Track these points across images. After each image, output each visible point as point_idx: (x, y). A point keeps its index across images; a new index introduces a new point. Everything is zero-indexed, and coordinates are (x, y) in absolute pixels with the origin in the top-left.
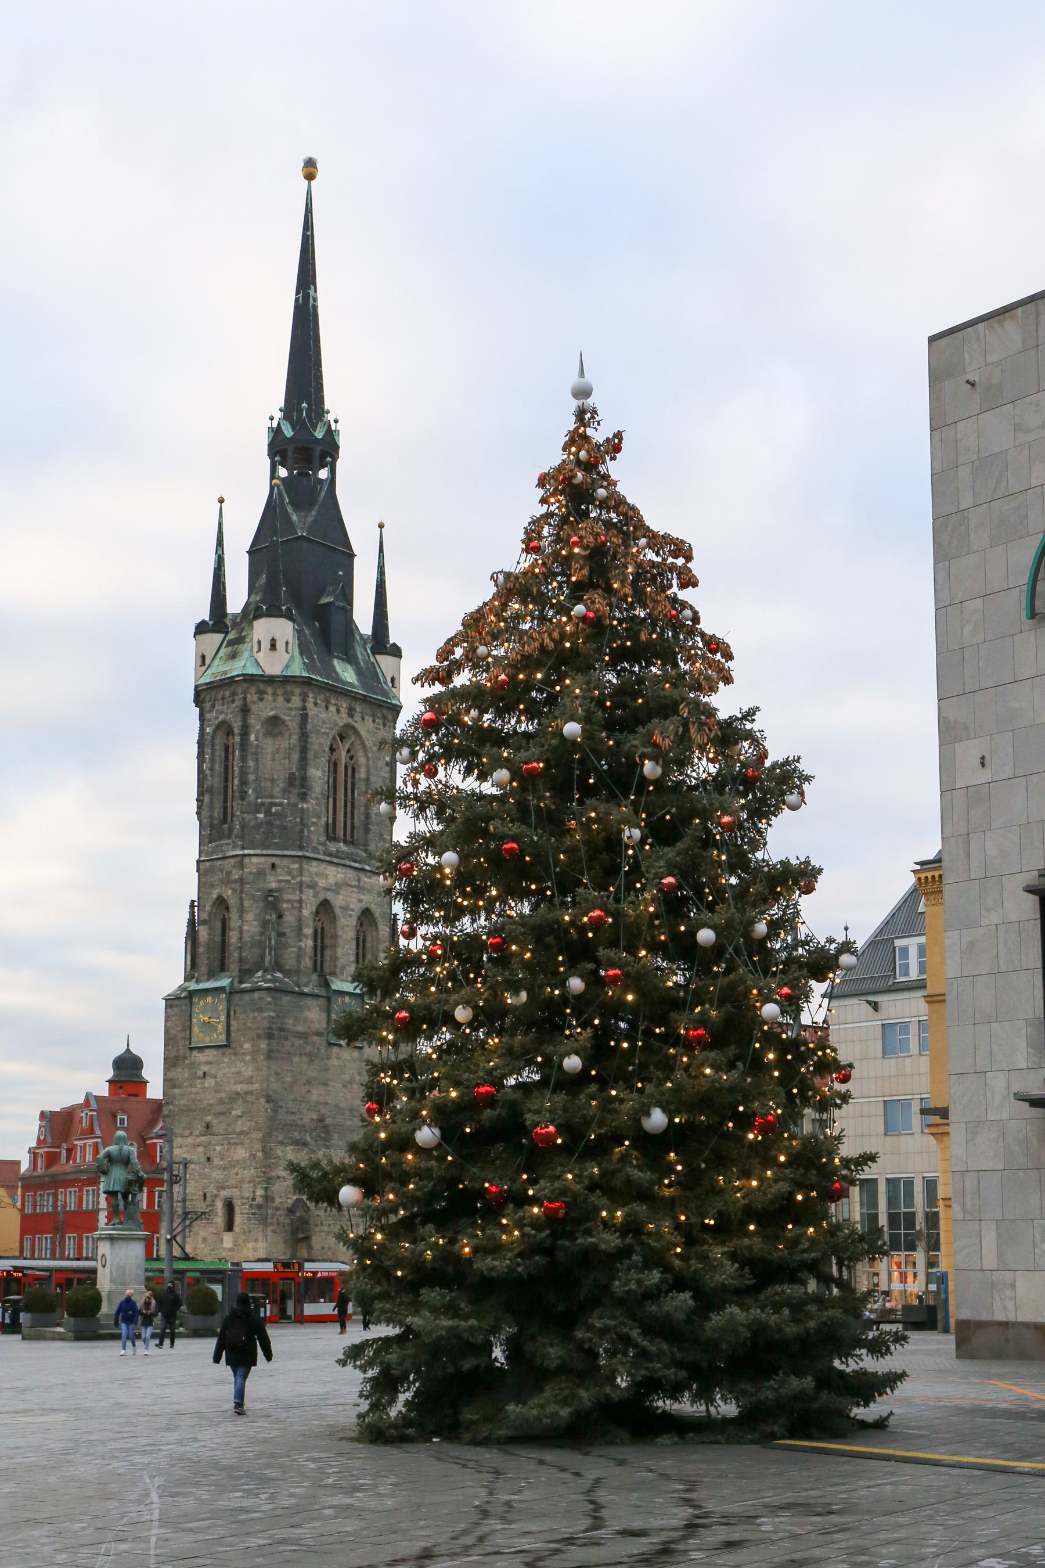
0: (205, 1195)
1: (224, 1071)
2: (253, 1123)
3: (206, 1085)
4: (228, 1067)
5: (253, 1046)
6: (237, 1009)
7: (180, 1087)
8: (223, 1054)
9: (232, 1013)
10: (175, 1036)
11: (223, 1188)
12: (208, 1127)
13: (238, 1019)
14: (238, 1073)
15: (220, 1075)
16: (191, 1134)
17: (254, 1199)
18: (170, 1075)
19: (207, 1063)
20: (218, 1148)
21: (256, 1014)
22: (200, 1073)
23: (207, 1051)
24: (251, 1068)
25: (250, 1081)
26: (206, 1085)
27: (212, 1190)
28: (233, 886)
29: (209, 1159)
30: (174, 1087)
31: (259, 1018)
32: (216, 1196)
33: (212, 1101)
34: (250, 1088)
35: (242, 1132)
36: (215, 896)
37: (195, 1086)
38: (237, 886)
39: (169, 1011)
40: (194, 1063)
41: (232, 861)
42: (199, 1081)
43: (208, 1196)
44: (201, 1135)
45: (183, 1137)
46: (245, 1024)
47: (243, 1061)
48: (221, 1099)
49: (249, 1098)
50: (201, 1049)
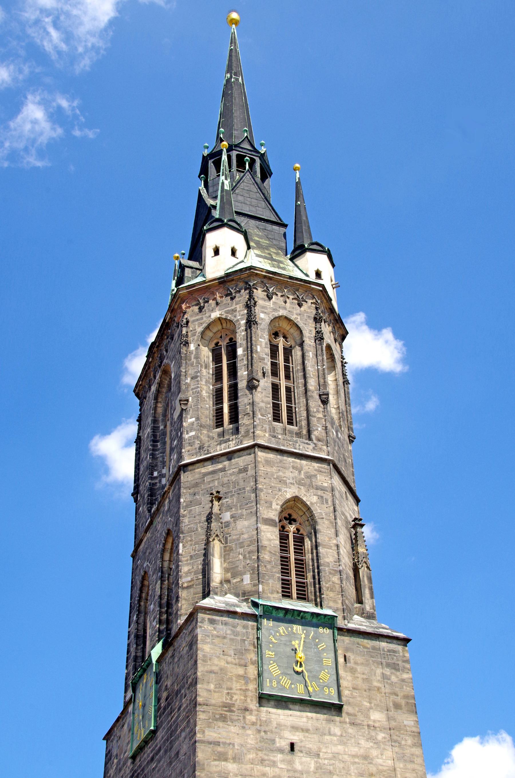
1: (335, 749)
4: (343, 743)
5: (389, 719)
7: (236, 759)
9: (341, 660)
13: (353, 671)
14: (365, 757)
15: (327, 752)
19: (295, 728)
21: (388, 671)
24: (389, 753)
26: (298, 766)
28: (320, 493)
30: (222, 757)
31: (394, 679)
36: (288, 496)
37: (274, 764)
38: (328, 496)
42: (279, 756)
46: (367, 680)
47: (371, 738)
50: (283, 702)
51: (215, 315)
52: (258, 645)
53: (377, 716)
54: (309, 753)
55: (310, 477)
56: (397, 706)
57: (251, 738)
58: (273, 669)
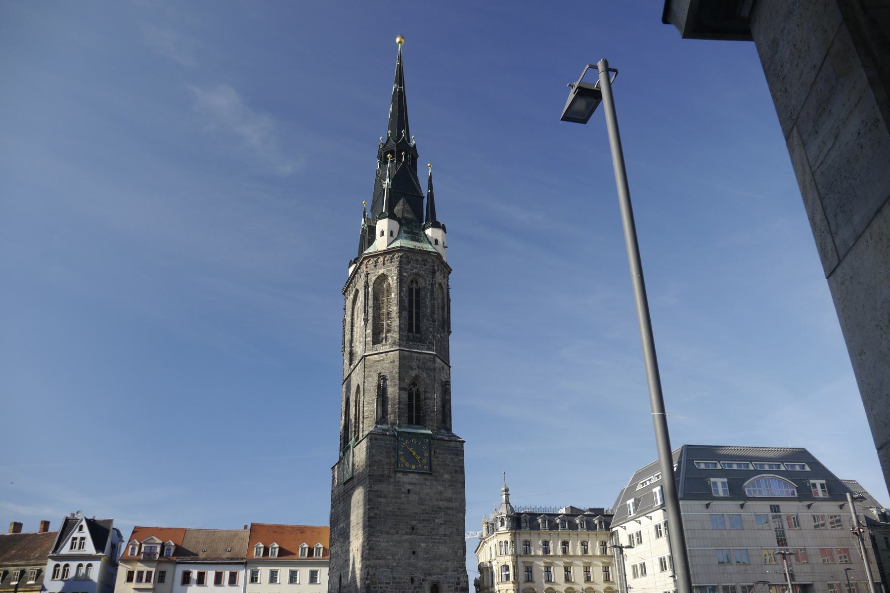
0: (412, 580)
2: (454, 530)
3: (411, 499)
6: (437, 451)
7: (385, 497)
8: (425, 479)
10: (380, 461)
11: (430, 575)
12: (413, 529)
13: (437, 457)
14: (441, 493)
16: (397, 532)
17: (458, 584)
18: (375, 488)
19: (410, 483)
20: (423, 545)
21: (453, 457)
22: (404, 490)
23: (411, 475)
25: (450, 500)
26: (411, 499)
27: (418, 575)
29: (414, 553)
30: (380, 496)
32: (424, 580)
33: (416, 511)
34: (451, 505)
35: (445, 535)
39: (373, 441)
40: (399, 482)
41: (427, 356)
43: (416, 579)
44: (406, 534)
45: (388, 533)
48: (424, 510)
49: (450, 512)
50: (405, 473)
51: (381, 271)
52: (396, 449)
53: (446, 476)
54: (416, 494)
55: (424, 363)
56: (456, 472)
57: (391, 488)
58: (402, 459)
